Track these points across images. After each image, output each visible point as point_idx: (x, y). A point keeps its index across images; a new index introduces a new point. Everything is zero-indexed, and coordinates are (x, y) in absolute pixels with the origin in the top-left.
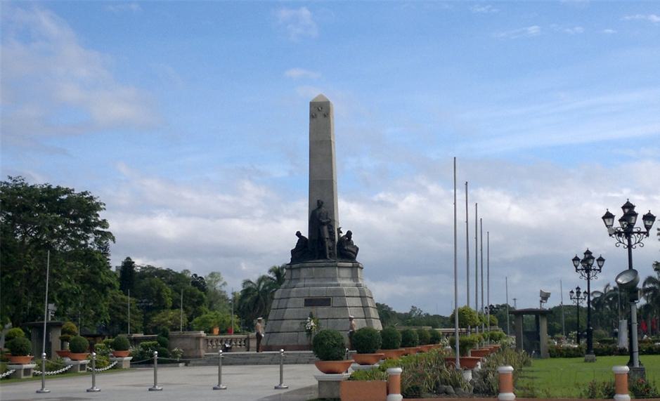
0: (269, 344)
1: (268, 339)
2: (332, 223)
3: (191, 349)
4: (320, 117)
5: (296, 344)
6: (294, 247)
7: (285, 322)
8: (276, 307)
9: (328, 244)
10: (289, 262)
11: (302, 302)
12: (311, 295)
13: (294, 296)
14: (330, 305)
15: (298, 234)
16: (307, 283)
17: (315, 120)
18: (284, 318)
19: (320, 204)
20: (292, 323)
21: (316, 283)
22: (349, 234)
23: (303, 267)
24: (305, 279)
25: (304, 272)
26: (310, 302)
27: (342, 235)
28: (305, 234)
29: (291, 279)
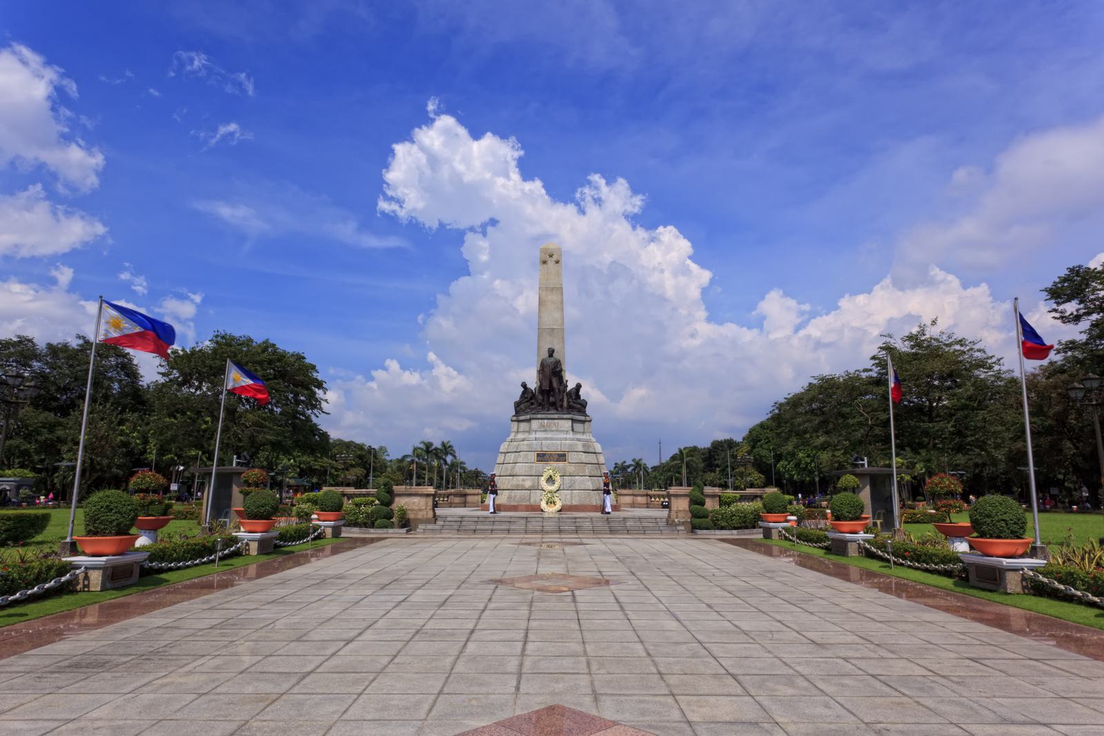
3: (420, 510)
4: (551, 263)
5: (528, 503)
6: (517, 398)
10: (514, 413)
11: (533, 456)
14: (565, 461)
15: (524, 385)
16: (539, 435)
17: (545, 266)
20: (523, 480)
21: (548, 436)
22: (579, 387)
24: (536, 431)
26: (542, 457)
27: (569, 389)
28: (533, 385)
29: (518, 432)
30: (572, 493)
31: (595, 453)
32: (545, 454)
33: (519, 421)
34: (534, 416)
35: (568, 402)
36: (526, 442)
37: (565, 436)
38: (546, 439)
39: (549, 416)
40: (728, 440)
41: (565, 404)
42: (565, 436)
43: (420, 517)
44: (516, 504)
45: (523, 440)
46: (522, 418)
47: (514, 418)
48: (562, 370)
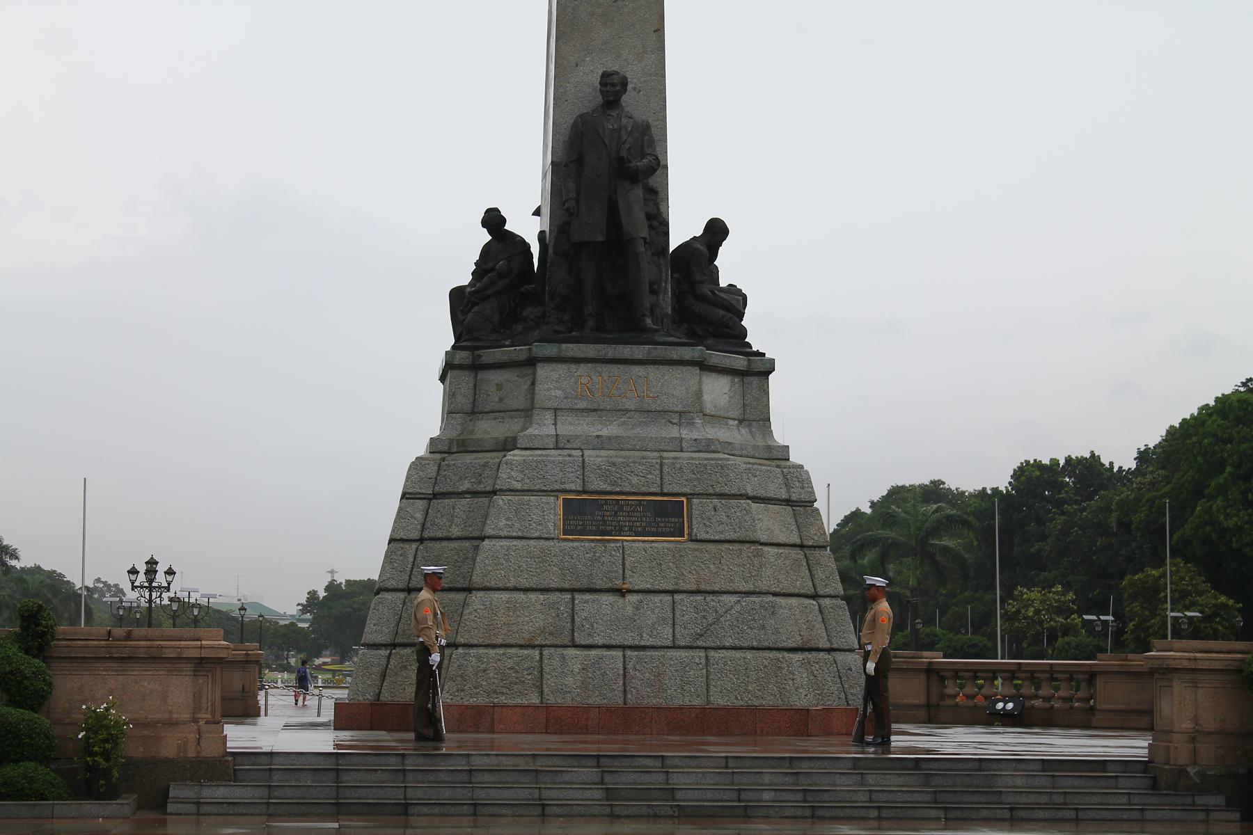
0: (386, 696)
1: (383, 677)
2: (653, 181)
3: (172, 724)
5: (535, 700)
6: (465, 279)
7: (477, 598)
8: (415, 535)
9: (647, 271)
12: (597, 484)
13: (518, 486)
15: (493, 220)
16: (570, 427)
18: (477, 579)
19: (613, 89)
21: (605, 432)
22: (716, 232)
23: (549, 360)
25: (553, 382)
26: (589, 513)
27: (674, 243)
30: (707, 657)
31: (788, 502)
32: (599, 505)
33: (476, 367)
34: (551, 350)
35: (679, 297)
36: (515, 456)
37: (674, 432)
38: (601, 443)
39: (611, 351)
40: (1081, 461)
41: (666, 301)
42: (674, 432)
43: (168, 749)
44: (481, 700)
45: (508, 445)
46: (490, 355)
47: (463, 357)
48: (657, 159)
